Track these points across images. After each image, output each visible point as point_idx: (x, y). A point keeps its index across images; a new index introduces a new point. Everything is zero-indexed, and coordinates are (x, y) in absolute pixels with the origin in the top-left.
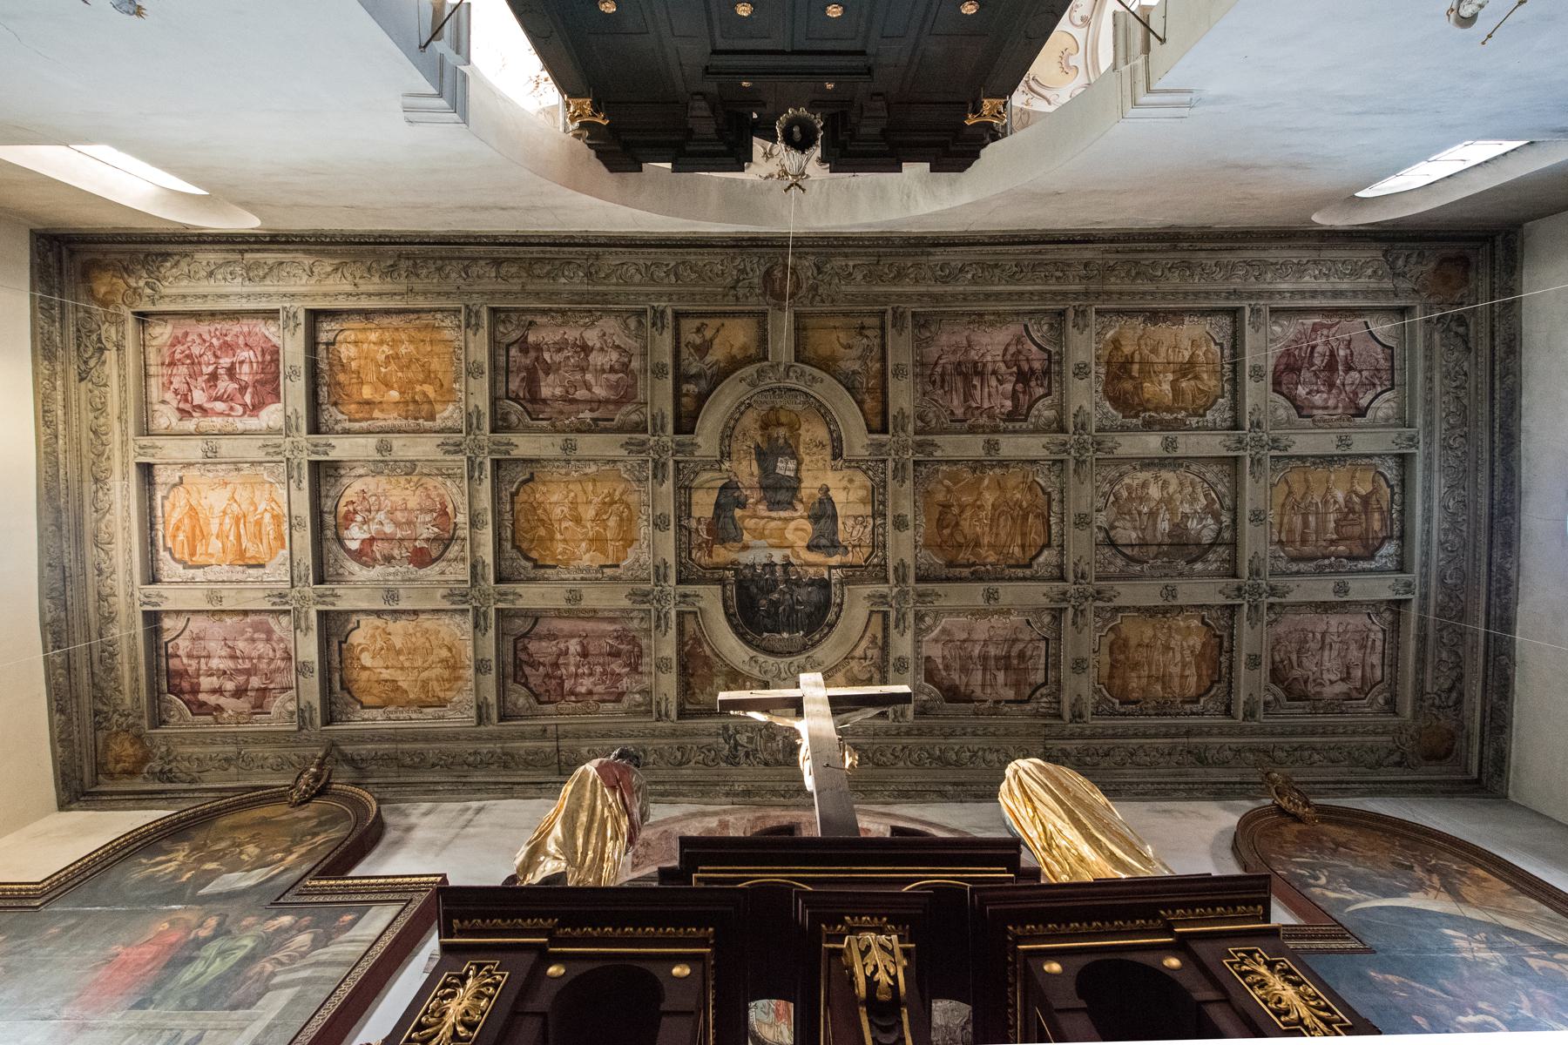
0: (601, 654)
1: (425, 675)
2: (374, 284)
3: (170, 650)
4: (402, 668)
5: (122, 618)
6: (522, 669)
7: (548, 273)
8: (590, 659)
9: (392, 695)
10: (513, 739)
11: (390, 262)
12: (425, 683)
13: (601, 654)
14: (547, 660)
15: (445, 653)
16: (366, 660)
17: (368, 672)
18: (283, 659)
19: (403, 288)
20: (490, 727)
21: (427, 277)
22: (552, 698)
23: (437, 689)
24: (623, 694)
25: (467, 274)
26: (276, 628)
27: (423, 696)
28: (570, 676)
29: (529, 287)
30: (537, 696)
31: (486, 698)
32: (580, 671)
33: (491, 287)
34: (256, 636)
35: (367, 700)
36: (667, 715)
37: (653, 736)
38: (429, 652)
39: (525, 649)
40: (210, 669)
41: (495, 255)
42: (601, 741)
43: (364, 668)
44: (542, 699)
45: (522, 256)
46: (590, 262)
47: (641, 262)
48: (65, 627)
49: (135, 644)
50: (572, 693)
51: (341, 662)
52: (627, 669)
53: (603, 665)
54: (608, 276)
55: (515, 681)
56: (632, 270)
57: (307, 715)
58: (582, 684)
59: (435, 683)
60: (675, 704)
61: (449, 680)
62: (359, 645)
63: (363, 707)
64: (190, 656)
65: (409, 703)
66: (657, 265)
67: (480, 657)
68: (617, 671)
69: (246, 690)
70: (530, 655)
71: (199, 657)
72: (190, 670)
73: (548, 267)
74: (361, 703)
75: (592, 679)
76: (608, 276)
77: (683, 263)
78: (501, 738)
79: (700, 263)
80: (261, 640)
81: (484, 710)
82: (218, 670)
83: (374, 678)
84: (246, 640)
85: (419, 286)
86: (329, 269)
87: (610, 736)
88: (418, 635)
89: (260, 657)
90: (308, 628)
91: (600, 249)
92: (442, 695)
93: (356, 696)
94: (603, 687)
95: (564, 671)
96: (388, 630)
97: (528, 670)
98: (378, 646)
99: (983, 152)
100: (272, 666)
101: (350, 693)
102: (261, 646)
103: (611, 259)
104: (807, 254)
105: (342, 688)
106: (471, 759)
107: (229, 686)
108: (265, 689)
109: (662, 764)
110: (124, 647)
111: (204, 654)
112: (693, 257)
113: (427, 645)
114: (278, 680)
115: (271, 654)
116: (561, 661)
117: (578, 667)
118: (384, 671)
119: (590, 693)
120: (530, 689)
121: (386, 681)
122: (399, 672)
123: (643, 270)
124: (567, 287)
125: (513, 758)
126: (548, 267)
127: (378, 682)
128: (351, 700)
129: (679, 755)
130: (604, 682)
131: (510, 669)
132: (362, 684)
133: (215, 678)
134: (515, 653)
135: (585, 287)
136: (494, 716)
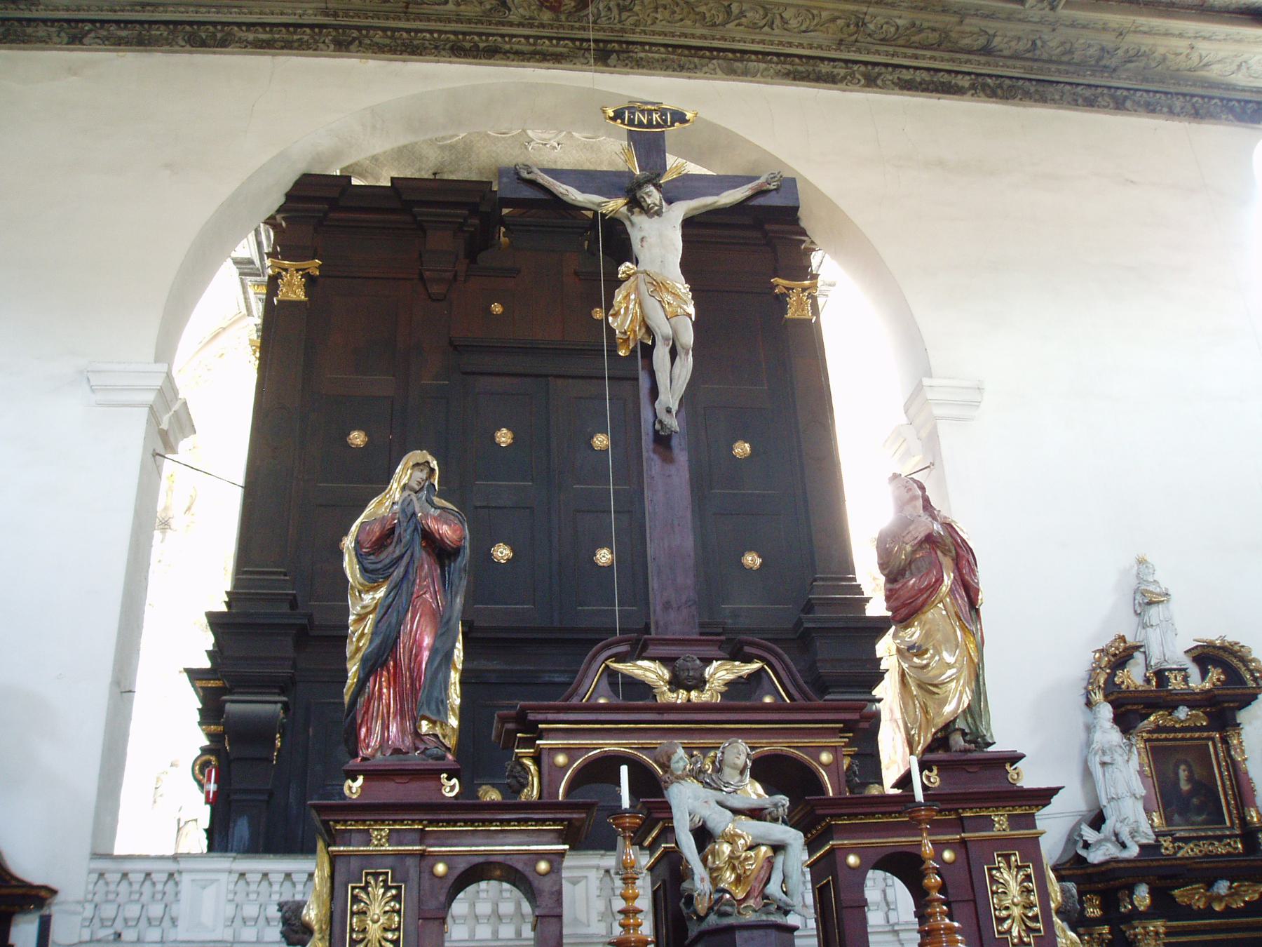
2: (1163, 46)
7: (921, 31)
11: (1130, 65)
19: (1130, 38)
21: (1090, 46)
25: (1034, 43)
29: (955, 19)
33: (1011, 25)
41: (983, 59)
45: (946, 55)
46: (854, 38)
47: (777, 31)
54: (834, 20)
56: (793, 23)
66: (754, 26)
73: (915, 38)
76: (834, 20)
77: (714, 25)
79: (689, 23)
85: (1108, 40)
86: (1214, 67)
91: (833, 54)
99: (282, 200)
103: (820, 42)
104: (520, 25)
112: (696, 34)
123: (778, 22)
124: (896, 13)
126: (913, 39)
135: (871, 10)
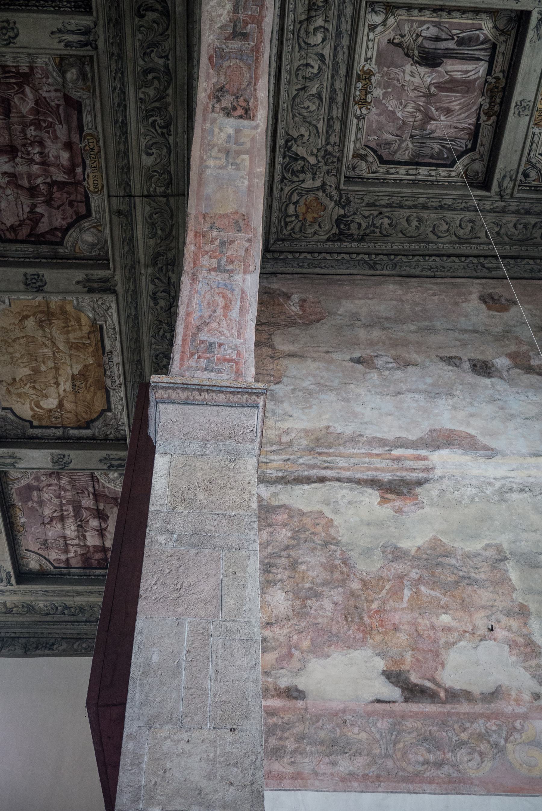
0: (8, 128)
1: (62, 346)
3: (62, 565)
4: (57, 369)
5: (28, 599)
6: (43, 235)
8: (18, 143)
9: (90, 381)
10: (132, 251)
12: (72, 346)
13: (8, 128)
14: (26, 202)
15: (31, 323)
16: (51, 403)
17: (65, 403)
18: (59, 478)
20: (118, 278)
22: (80, 197)
23: (79, 334)
24: (67, 98)
26: (24, 482)
27: (90, 349)
28: (46, 173)
30: (80, 218)
31: (78, 283)
32: (37, 158)
34: (36, 499)
35: (99, 405)
36: (86, 32)
37: (120, 57)
38: (31, 339)
39: (12, 228)
40: (77, 537)
42: (133, 137)
43: (61, 405)
44: (83, 209)
48: (34, 640)
49: (52, 591)
50: (71, 171)
51: (56, 428)
52: (27, 90)
53: (25, 126)
55: (61, 243)
57: (115, 463)
58: (57, 157)
59: (72, 336)
60: (66, 19)
61: (66, 321)
62: (32, 409)
63: (109, 409)
64: (66, 551)
65: (100, 365)
67: (22, 287)
68: (31, 104)
69: (98, 510)
70: (22, 223)
71: (66, 545)
72: (80, 551)
74: (103, 411)
75: (48, 143)
78: (132, 267)
80: (39, 496)
81: (95, 285)
82: (77, 531)
83: (71, 398)
84: (41, 507)
87: (124, 124)
88: (11, 350)
89: (59, 497)
90: (12, 456)
92: (86, 329)
93: (94, 416)
94: (58, 127)
95: (39, 181)
96: (10, 381)
97: (43, 227)
98: (31, 391)
100: (69, 487)
101: (93, 421)
102: (46, 496)
105: (88, 428)
106: (162, 303)
107: (94, 523)
108: (95, 494)
109: (166, 45)
110: (57, 600)
111: (62, 541)
113: (22, 341)
114: (83, 483)
115: (56, 488)
116: (25, 183)
117: (31, 161)
118: (62, 387)
119: (69, 146)
120: (70, 226)
121: (74, 386)
122: (61, 372)
125: (159, 254)
127: (76, 393)
128: (101, 420)
129: (151, 16)
130: (51, 125)
131: (44, 249)
132: (81, 409)
133: (87, 534)
134: (22, 242)
136: (101, 273)
